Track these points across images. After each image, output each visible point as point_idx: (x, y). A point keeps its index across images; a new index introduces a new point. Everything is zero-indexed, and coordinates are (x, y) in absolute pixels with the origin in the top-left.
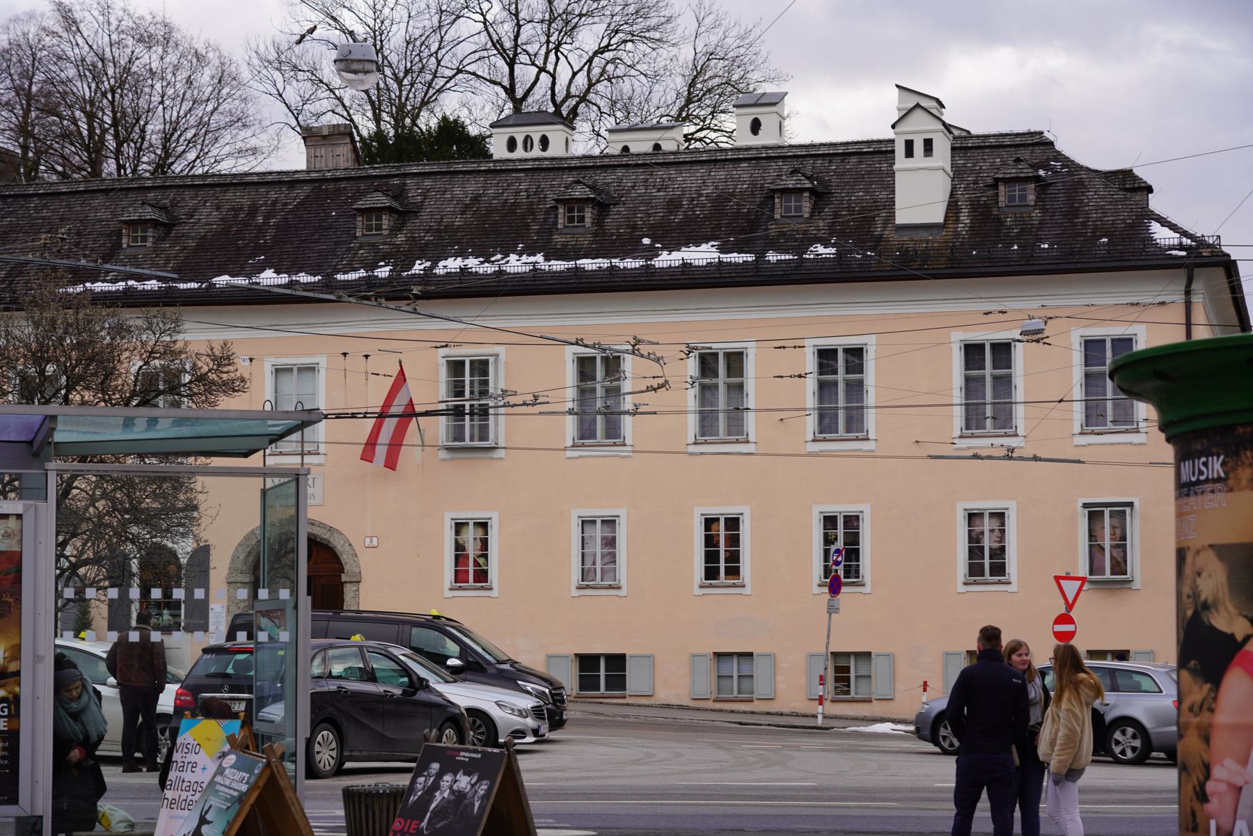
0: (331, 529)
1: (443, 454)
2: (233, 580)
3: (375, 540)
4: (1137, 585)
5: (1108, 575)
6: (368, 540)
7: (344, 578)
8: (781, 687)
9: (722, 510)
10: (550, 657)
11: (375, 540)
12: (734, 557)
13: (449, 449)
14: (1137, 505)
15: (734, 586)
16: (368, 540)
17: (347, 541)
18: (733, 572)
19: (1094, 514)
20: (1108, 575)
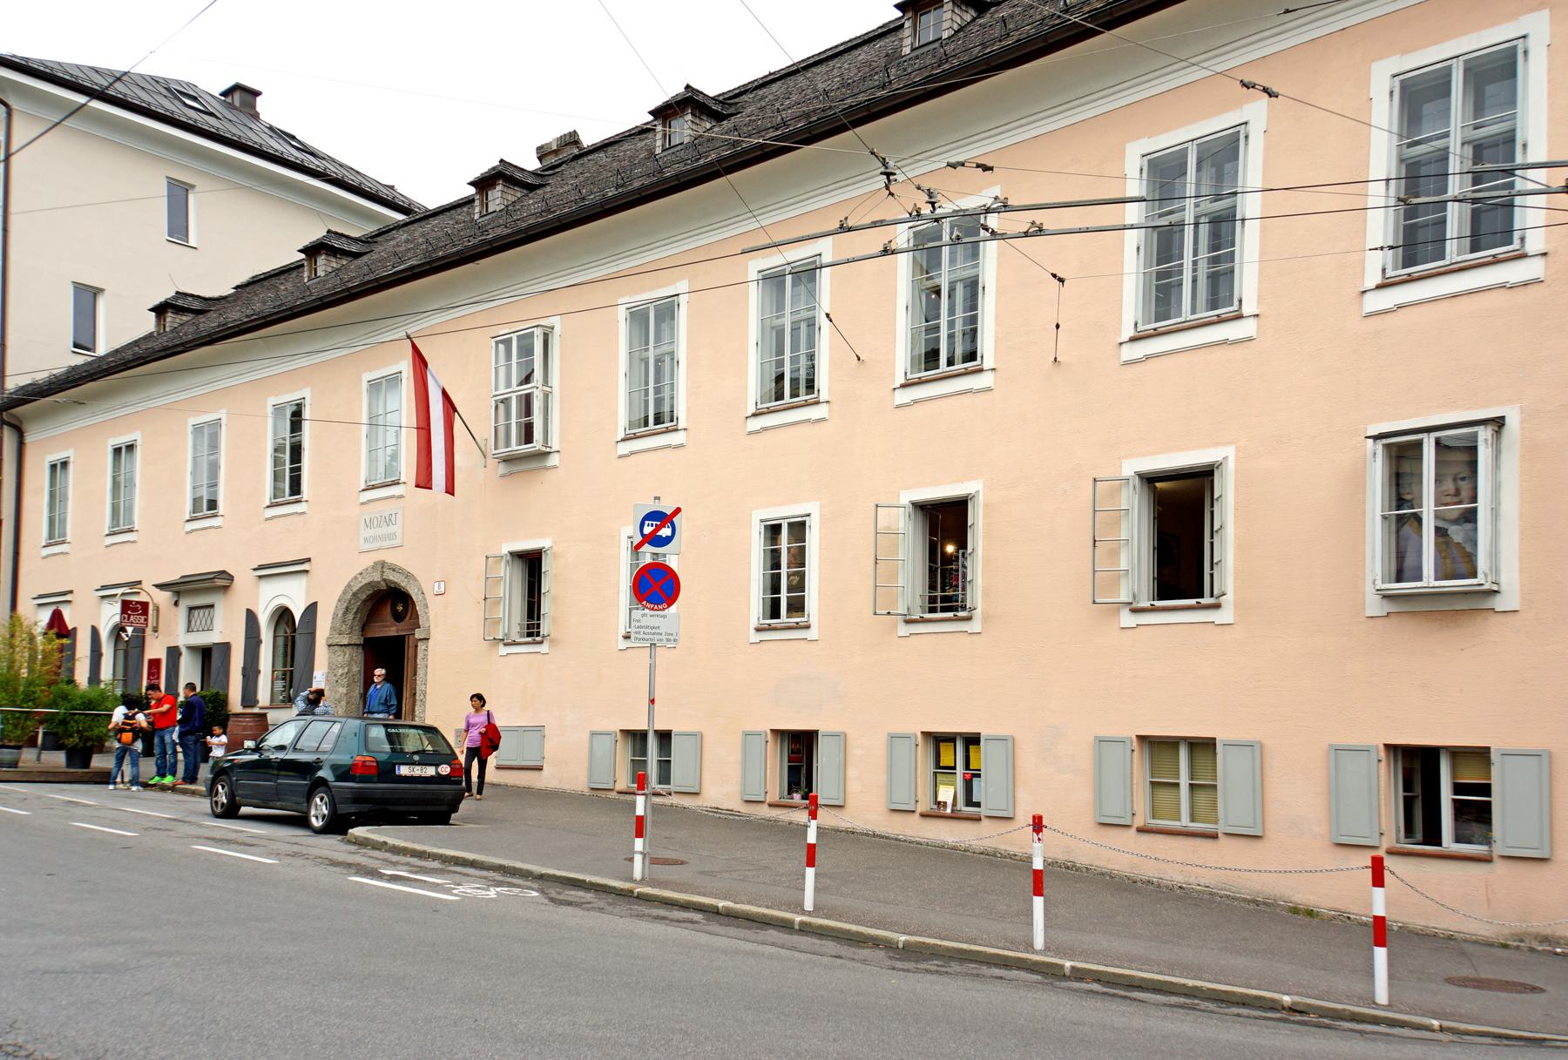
0: (408, 575)
1: (502, 469)
2: (335, 641)
4: (1508, 599)
5: (1429, 580)
8: (853, 786)
9: (784, 512)
10: (593, 734)
12: (798, 585)
13: (508, 460)
14: (1513, 422)
15: (798, 627)
17: (420, 588)
18: (797, 606)
19: (1401, 455)
20: (1429, 580)
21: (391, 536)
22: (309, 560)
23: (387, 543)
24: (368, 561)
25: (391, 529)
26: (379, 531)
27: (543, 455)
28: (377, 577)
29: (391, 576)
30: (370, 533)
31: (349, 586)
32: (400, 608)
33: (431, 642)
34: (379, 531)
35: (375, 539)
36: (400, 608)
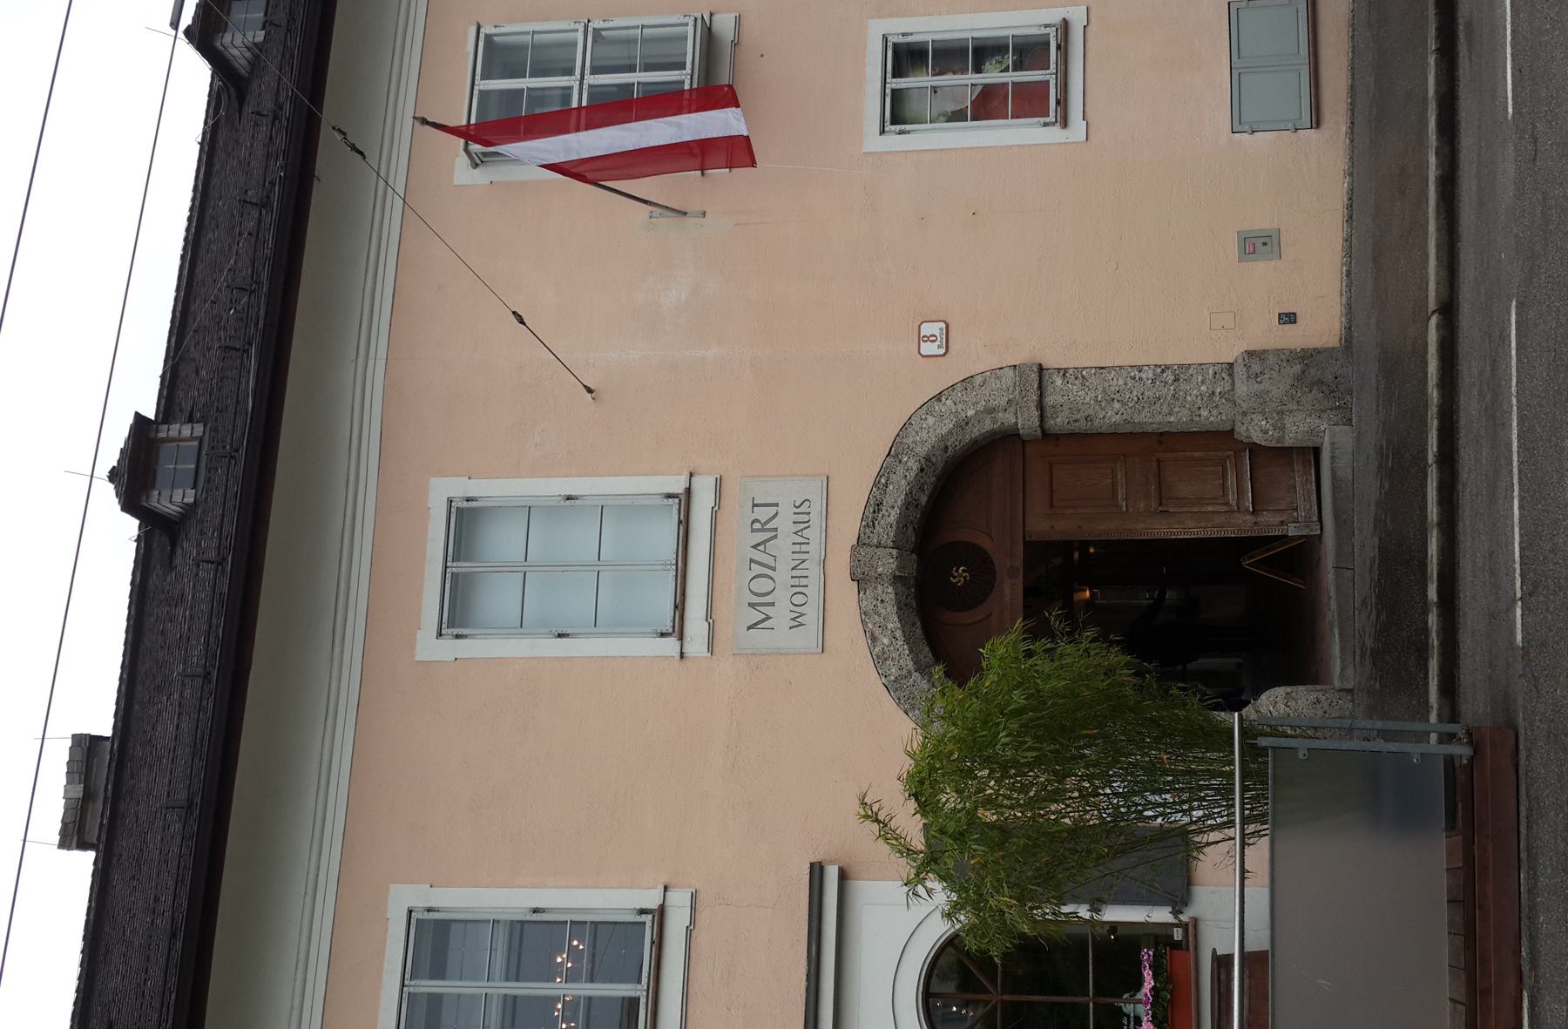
3: (927, 329)
6: (928, 348)
7: (1027, 421)
11: (927, 329)
16: (928, 348)
21: (802, 525)
22: (817, 872)
23: (814, 534)
24: (845, 594)
25: (784, 523)
26: (783, 574)
27: (709, 37)
28: (887, 563)
29: (891, 515)
30: (781, 613)
31: (894, 687)
32: (960, 575)
33: (1051, 361)
34: (783, 574)
35: (799, 589)
36: (960, 575)
